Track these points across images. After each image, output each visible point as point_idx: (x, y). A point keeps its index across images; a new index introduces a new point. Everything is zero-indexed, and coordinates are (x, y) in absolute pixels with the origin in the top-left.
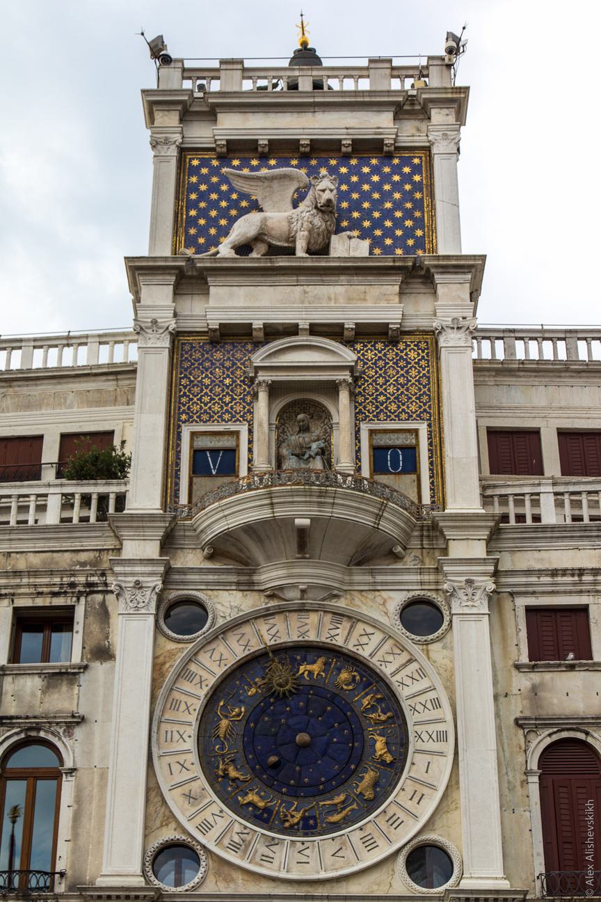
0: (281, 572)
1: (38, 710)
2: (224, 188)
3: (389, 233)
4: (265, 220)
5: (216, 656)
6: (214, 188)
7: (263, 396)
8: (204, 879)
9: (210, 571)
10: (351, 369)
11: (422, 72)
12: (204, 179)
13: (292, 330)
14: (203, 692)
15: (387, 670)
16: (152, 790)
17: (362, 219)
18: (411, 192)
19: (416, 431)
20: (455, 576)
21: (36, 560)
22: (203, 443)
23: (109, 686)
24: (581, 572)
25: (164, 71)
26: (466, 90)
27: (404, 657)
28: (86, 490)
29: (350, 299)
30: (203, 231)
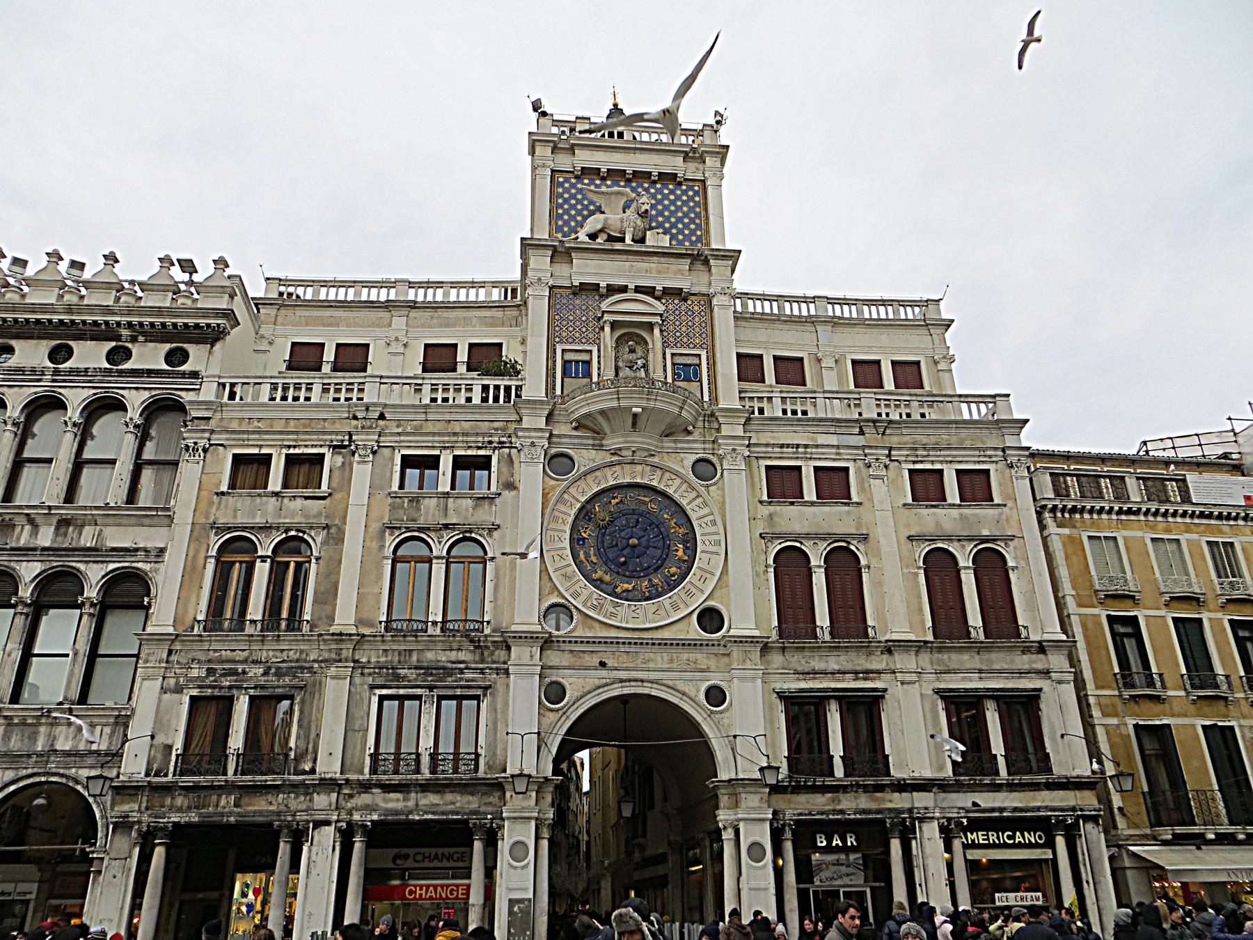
0: (621, 440)
1: (471, 520)
2: (579, 197)
3: (681, 232)
4: (606, 220)
5: (580, 490)
6: (573, 197)
7: (607, 329)
8: (576, 627)
9: (576, 437)
10: (661, 315)
11: (700, 133)
12: (567, 190)
13: (624, 289)
15: (684, 502)
16: (544, 570)
17: (664, 222)
18: (693, 207)
19: (699, 356)
20: (724, 447)
21: (466, 425)
22: (569, 356)
24: (798, 446)
25: (542, 120)
26: (728, 147)
27: (694, 494)
28: (497, 383)
29: (659, 272)
30: (566, 223)
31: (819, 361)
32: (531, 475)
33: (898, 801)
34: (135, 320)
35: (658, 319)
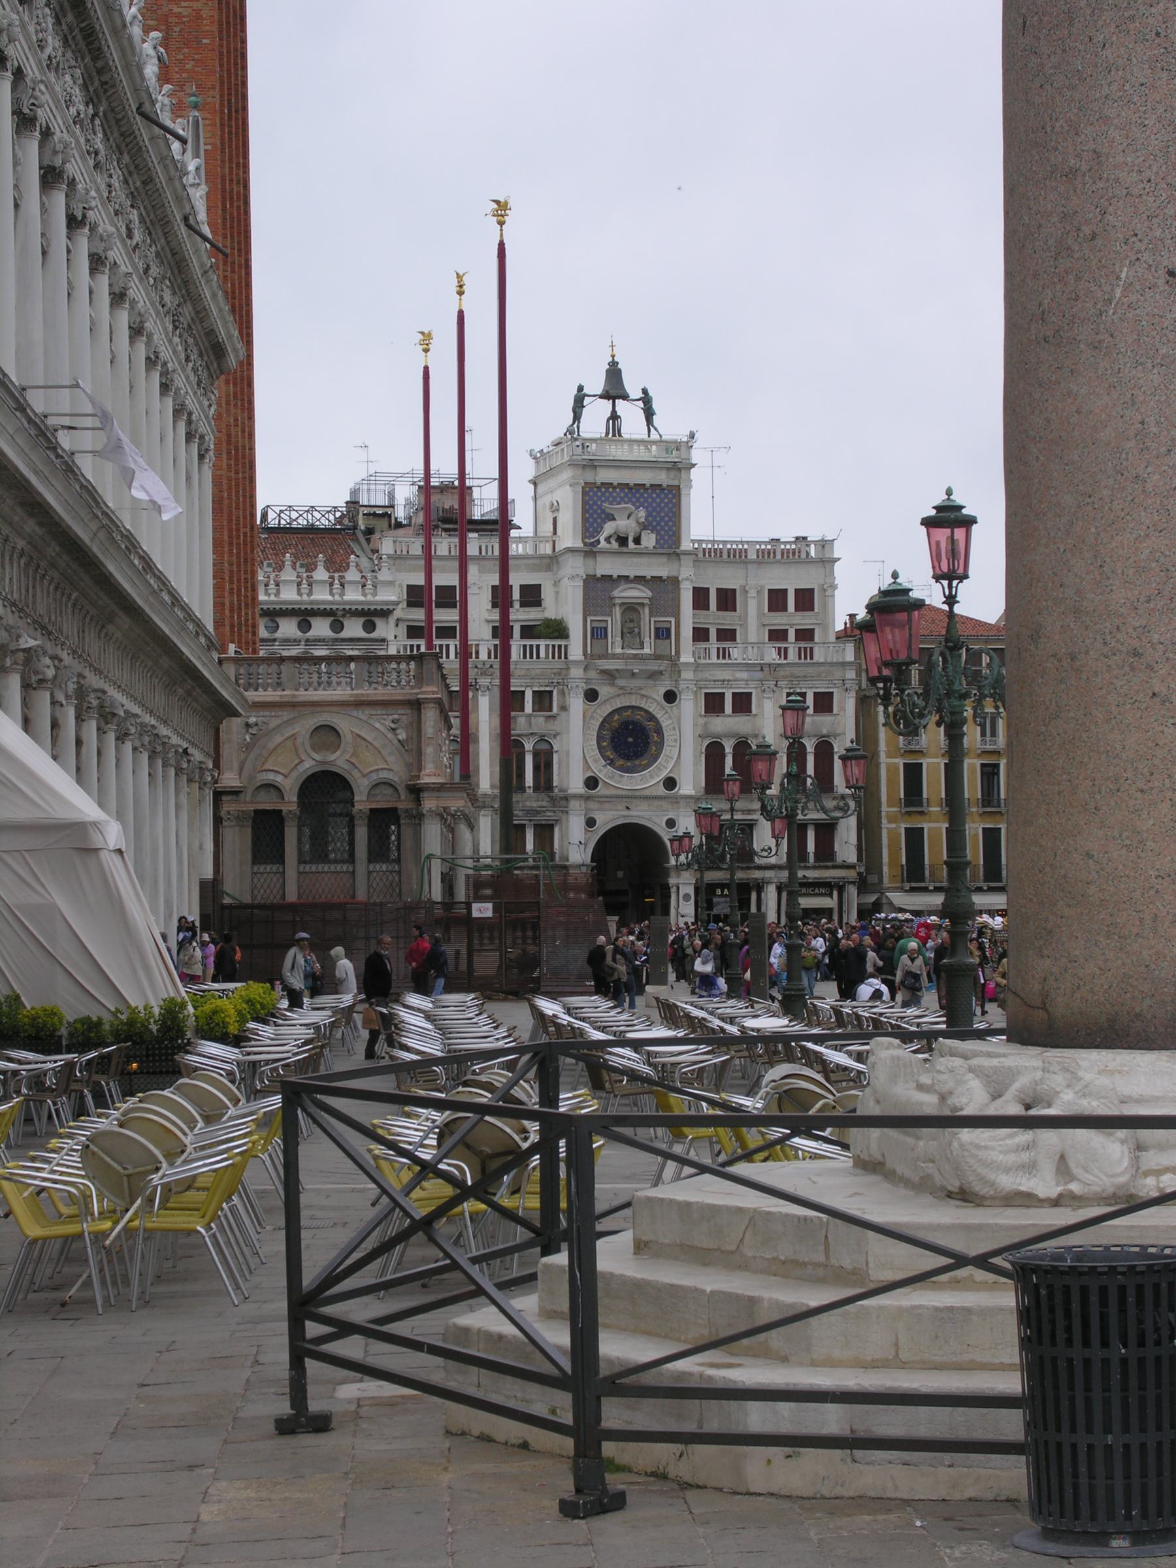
7: (618, 608)
14: (598, 724)
15: (658, 716)
20: (682, 686)
21: (538, 672)
22: (596, 625)
23: (568, 721)
30: (591, 525)
31: (747, 592)
32: (577, 703)
33: (757, 874)
34: (347, 607)
35: (646, 601)
